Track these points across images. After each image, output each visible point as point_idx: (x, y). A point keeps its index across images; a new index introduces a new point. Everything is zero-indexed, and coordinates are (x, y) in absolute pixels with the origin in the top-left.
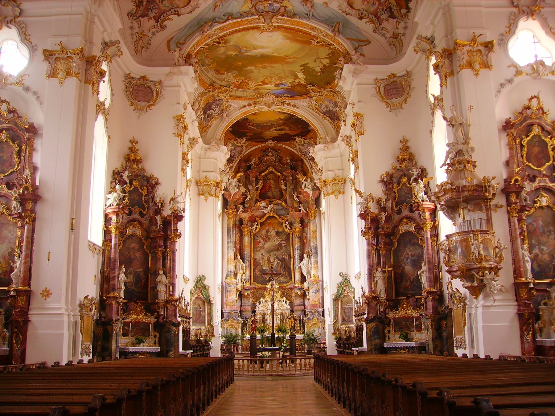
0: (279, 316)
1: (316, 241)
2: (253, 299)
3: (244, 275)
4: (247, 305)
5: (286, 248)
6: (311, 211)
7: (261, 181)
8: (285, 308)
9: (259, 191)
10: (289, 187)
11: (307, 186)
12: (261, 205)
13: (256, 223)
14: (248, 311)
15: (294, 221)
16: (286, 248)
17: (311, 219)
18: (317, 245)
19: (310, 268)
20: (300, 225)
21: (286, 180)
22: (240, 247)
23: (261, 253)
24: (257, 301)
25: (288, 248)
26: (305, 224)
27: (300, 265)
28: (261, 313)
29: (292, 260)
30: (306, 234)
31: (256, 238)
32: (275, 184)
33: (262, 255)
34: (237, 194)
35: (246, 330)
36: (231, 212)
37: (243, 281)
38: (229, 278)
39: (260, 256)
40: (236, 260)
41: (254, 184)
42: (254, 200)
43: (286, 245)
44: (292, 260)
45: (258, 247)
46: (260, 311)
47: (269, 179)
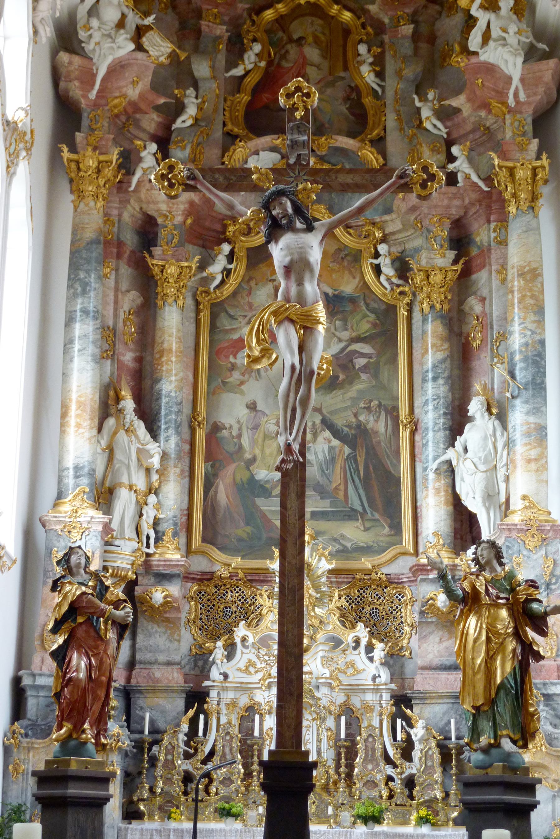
0: (330, 722)
1: (540, 322)
2: (195, 630)
3: (152, 499)
4: (162, 658)
5: (376, 375)
6: (511, 171)
7: (257, 48)
8: (366, 679)
9: (245, 98)
10: (399, 74)
11: (495, 32)
12: (252, 163)
13: (226, 248)
14: (168, 691)
15: (418, 242)
16: (376, 375)
17: (512, 209)
18: (542, 343)
19: (501, 473)
20: (451, 255)
21: (382, 44)
22: (139, 360)
23: (249, 398)
24: (216, 638)
25: (385, 374)
26: (474, 251)
27: (450, 454)
28: (233, 704)
29: (405, 435)
30: (483, 300)
31: (224, 323)
32: (325, 65)
33: (252, 407)
34: (130, 74)
35: (152, 790)
36: (91, 162)
37: (147, 530)
38: (66, 507)
39: (243, 412)
40: (111, 422)
41: (221, 59)
42: (218, 134)
43: (377, 363)
44: (405, 435)
45: (233, 367)
46: (230, 695)
47: (300, 41)
